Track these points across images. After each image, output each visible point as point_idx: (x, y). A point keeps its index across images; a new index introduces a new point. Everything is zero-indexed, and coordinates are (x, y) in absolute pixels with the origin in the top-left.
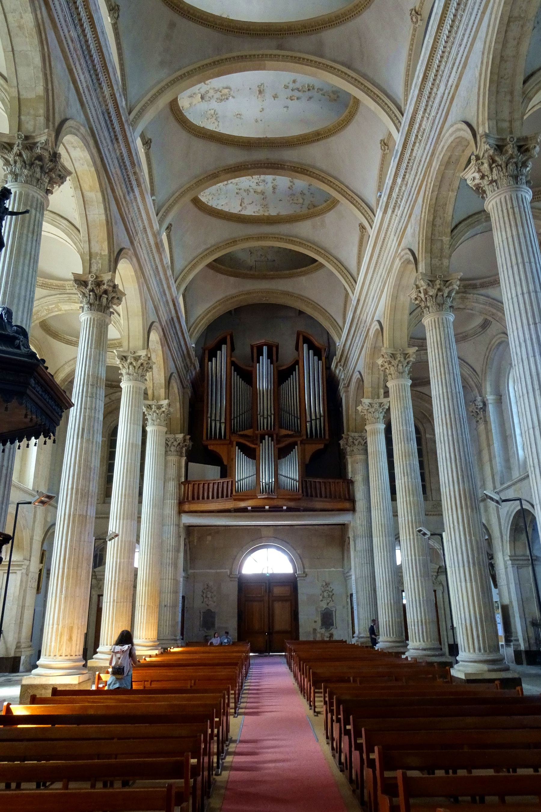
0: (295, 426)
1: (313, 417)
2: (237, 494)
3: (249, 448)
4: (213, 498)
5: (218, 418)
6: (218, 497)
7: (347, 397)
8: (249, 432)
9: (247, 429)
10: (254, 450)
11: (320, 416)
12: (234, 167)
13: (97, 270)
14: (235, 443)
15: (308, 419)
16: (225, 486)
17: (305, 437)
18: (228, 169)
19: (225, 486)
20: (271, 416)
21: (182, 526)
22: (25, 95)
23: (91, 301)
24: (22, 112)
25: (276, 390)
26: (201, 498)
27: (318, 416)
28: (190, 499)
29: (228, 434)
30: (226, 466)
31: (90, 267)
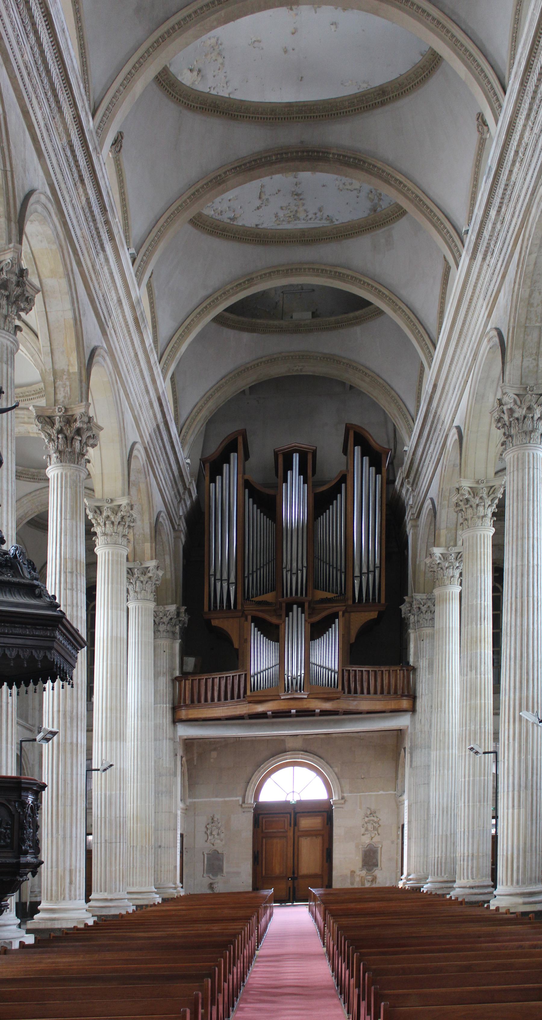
0: (337, 585)
1: (365, 570)
2: (254, 694)
3: (271, 624)
4: (219, 699)
6: (226, 699)
7: (415, 535)
8: (269, 597)
10: (277, 627)
11: (375, 567)
12: (250, 162)
13: (65, 397)
14: (249, 618)
15: (357, 573)
16: (236, 682)
17: (350, 602)
18: (240, 166)
19: (236, 682)
20: (302, 571)
23: (60, 448)
27: (371, 568)
30: (237, 650)
31: (55, 393)
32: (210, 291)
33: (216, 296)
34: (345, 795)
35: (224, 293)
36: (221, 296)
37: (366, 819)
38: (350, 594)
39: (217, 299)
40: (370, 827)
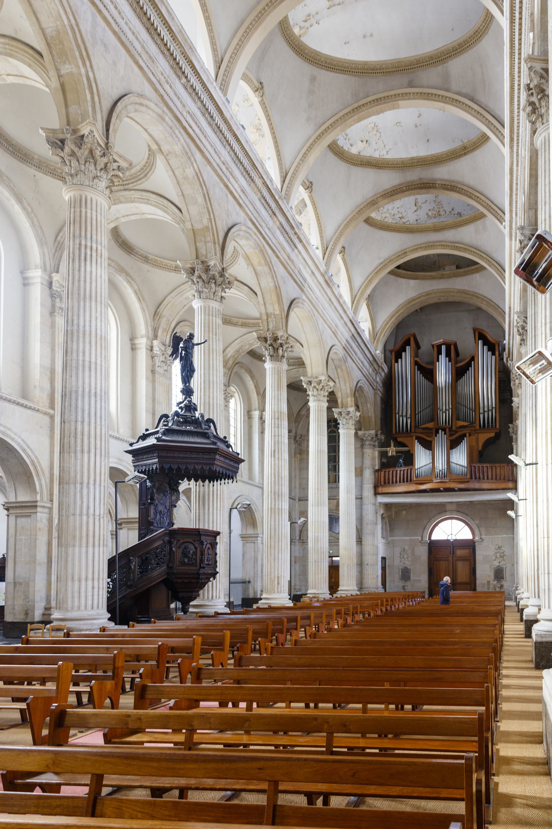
1: (486, 409)
3: (428, 441)
5: (404, 414)
8: (430, 425)
9: (429, 422)
11: (492, 408)
15: (481, 411)
17: (478, 427)
20: (449, 410)
21: (378, 504)
22: (197, 226)
24: (197, 240)
25: (453, 385)
26: (391, 482)
27: (490, 408)
28: (382, 483)
29: (413, 428)
32: (382, 260)
33: (385, 263)
34: (483, 537)
35: (390, 261)
36: (388, 262)
37: (496, 551)
38: (478, 423)
39: (386, 264)
40: (498, 555)
